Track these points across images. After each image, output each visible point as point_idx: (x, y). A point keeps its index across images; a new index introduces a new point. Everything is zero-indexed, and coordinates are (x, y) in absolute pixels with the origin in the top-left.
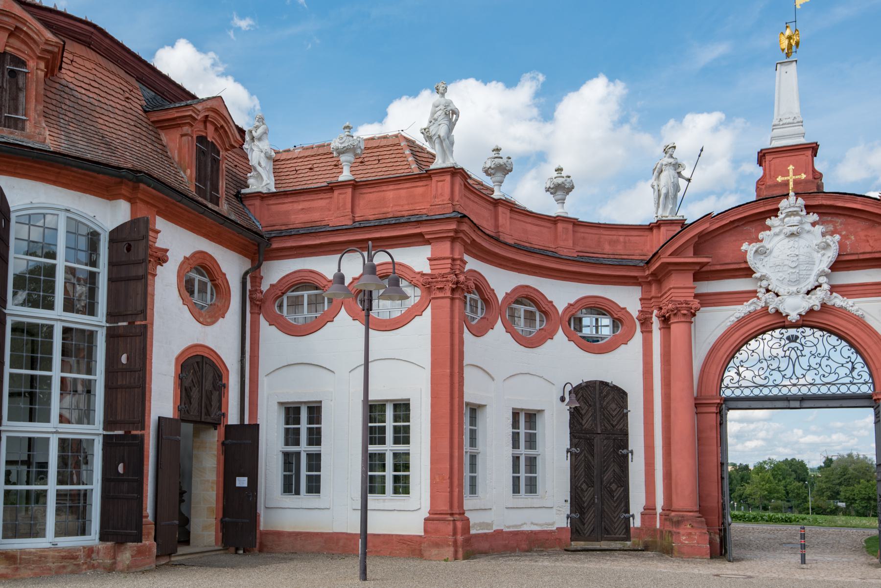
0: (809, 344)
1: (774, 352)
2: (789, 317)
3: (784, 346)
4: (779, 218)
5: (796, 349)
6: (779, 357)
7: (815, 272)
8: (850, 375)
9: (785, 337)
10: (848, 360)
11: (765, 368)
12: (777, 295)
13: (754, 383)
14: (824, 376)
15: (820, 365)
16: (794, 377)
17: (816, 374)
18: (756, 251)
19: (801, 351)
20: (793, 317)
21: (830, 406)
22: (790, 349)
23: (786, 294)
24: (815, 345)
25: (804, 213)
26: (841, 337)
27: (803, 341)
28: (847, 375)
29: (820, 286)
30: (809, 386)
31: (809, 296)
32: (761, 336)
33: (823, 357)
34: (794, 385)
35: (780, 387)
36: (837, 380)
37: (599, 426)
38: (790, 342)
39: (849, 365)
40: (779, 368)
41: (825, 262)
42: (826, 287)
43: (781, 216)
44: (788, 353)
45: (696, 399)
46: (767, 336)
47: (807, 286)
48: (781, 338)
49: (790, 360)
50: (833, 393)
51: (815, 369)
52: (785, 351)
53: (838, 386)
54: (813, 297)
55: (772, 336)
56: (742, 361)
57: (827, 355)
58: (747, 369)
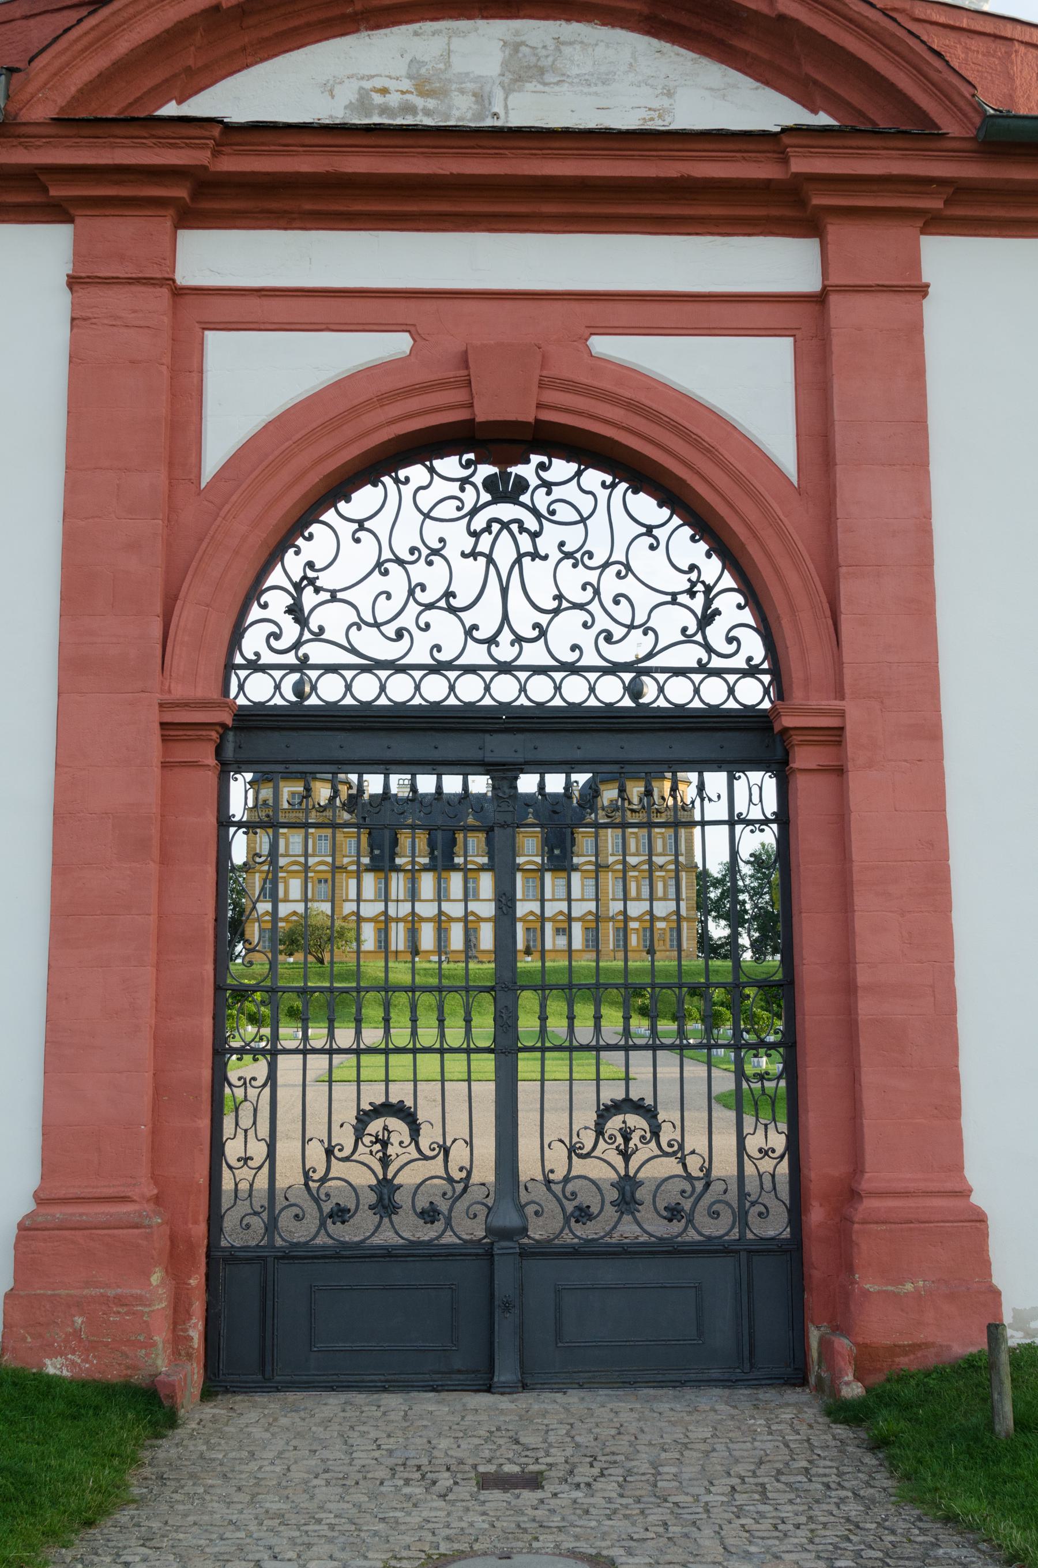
0: (564, 513)
5: (514, 527)
8: (699, 638)
9: (478, 479)
13: (353, 651)
14: (609, 638)
15: (597, 592)
19: (535, 535)
22: (496, 527)
24: (583, 520)
27: (542, 501)
28: (687, 638)
30: (558, 676)
34: (505, 668)
35: (452, 675)
38: (494, 501)
44: (486, 541)
46: (417, 473)
48: (464, 482)
49: (492, 568)
51: (581, 607)
55: (432, 470)
56: (310, 565)
58: (334, 599)
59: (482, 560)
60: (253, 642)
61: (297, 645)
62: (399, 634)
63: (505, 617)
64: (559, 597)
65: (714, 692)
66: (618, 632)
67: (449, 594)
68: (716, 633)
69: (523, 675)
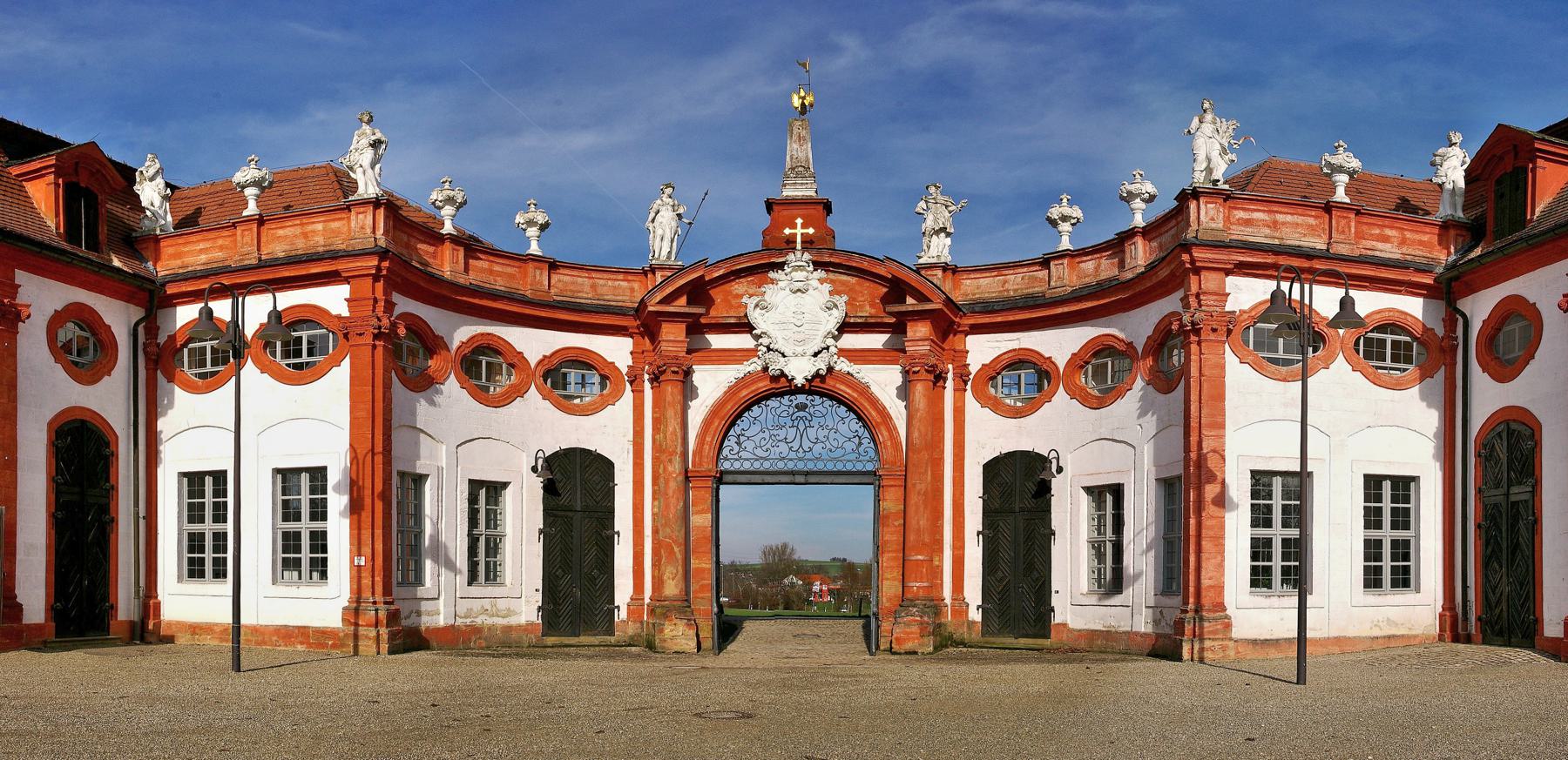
0: (818, 414)
1: (782, 421)
3: (793, 414)
9: (794, 405)
11: (768, 439)
12: (784, 356)
13: (755, 454)
14: (831, 451)
21: (835, 481)
25: (811, 268)
27: (812, 410)
32: (764, 403)
33: (831, 430)
34: (800, 459)
37: (579, 502)
44: (796, 422)
55: (780, 402)
60: (725, 452)
61: (738, 453)
63: (801, 445)
65: (859, 467)
66: (833, 449)
67: (786, 439)
68: (861, 449)
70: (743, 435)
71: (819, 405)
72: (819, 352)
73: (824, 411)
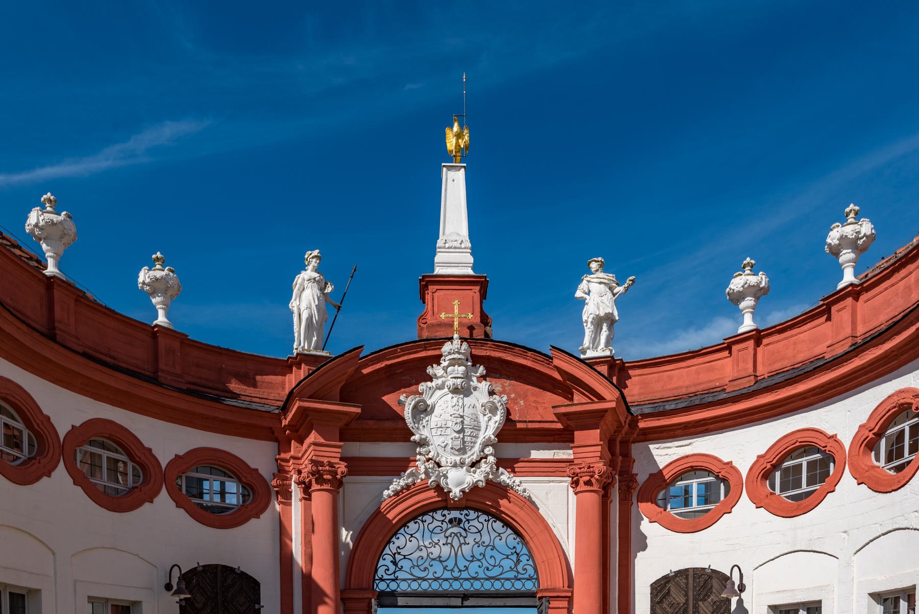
2: (451, 494)
4: (442, 365)
5: (459, 535)
6: (441, 543)
7: (480, 440)
9: (447, 520)
10: (514, 551)
12: (439, 466)
13: (412, 574)
14: (488, 569)
16: (456, 569)
17: (479, 566)
18: (415, 407)
20: (456, 492)
21: (493, 604)
22: (453, 535)
23: (449, 464)
24: (479, 532)
26: (507, 524)
29: (486, 457)
30: (472, 581)
31: (474, 469)
32: (420, 518)
33: (487, 546)
34: (456, 579)
35: (440, 581)
36: (501, 574)
39: (514, 557)
40: (440, 557)
41: (492, 428)
42: (491, 459)
43: (445, 364)
44: (449, 541)
45: (342, 592)
46: (428, 518)
47: (472, 457)
48: (443, 521)
50: (497, 590)
51: (479, 560)
52: (447, 537)
53: (503, 581)
54: (478, 471)
55: (433, 517)
56: (399, 547)
57: (491, 544)
58: (405, 558)
59: (449, 545)
62: (425, 570)
63: (456, 564)
64: (473, 556)
66: (491, 567)
69: (461, 581)
70: (399, 553)
71: (477, 520)
72: (478, 462)
73: (480, 526)
